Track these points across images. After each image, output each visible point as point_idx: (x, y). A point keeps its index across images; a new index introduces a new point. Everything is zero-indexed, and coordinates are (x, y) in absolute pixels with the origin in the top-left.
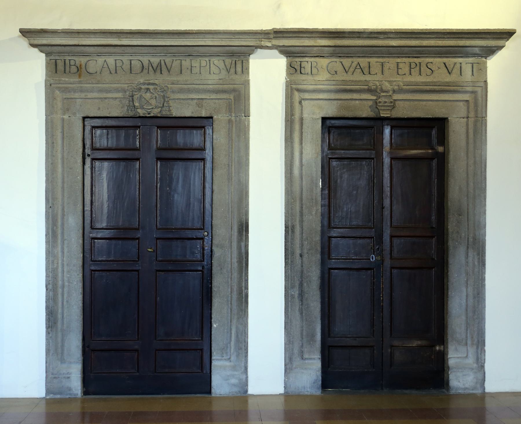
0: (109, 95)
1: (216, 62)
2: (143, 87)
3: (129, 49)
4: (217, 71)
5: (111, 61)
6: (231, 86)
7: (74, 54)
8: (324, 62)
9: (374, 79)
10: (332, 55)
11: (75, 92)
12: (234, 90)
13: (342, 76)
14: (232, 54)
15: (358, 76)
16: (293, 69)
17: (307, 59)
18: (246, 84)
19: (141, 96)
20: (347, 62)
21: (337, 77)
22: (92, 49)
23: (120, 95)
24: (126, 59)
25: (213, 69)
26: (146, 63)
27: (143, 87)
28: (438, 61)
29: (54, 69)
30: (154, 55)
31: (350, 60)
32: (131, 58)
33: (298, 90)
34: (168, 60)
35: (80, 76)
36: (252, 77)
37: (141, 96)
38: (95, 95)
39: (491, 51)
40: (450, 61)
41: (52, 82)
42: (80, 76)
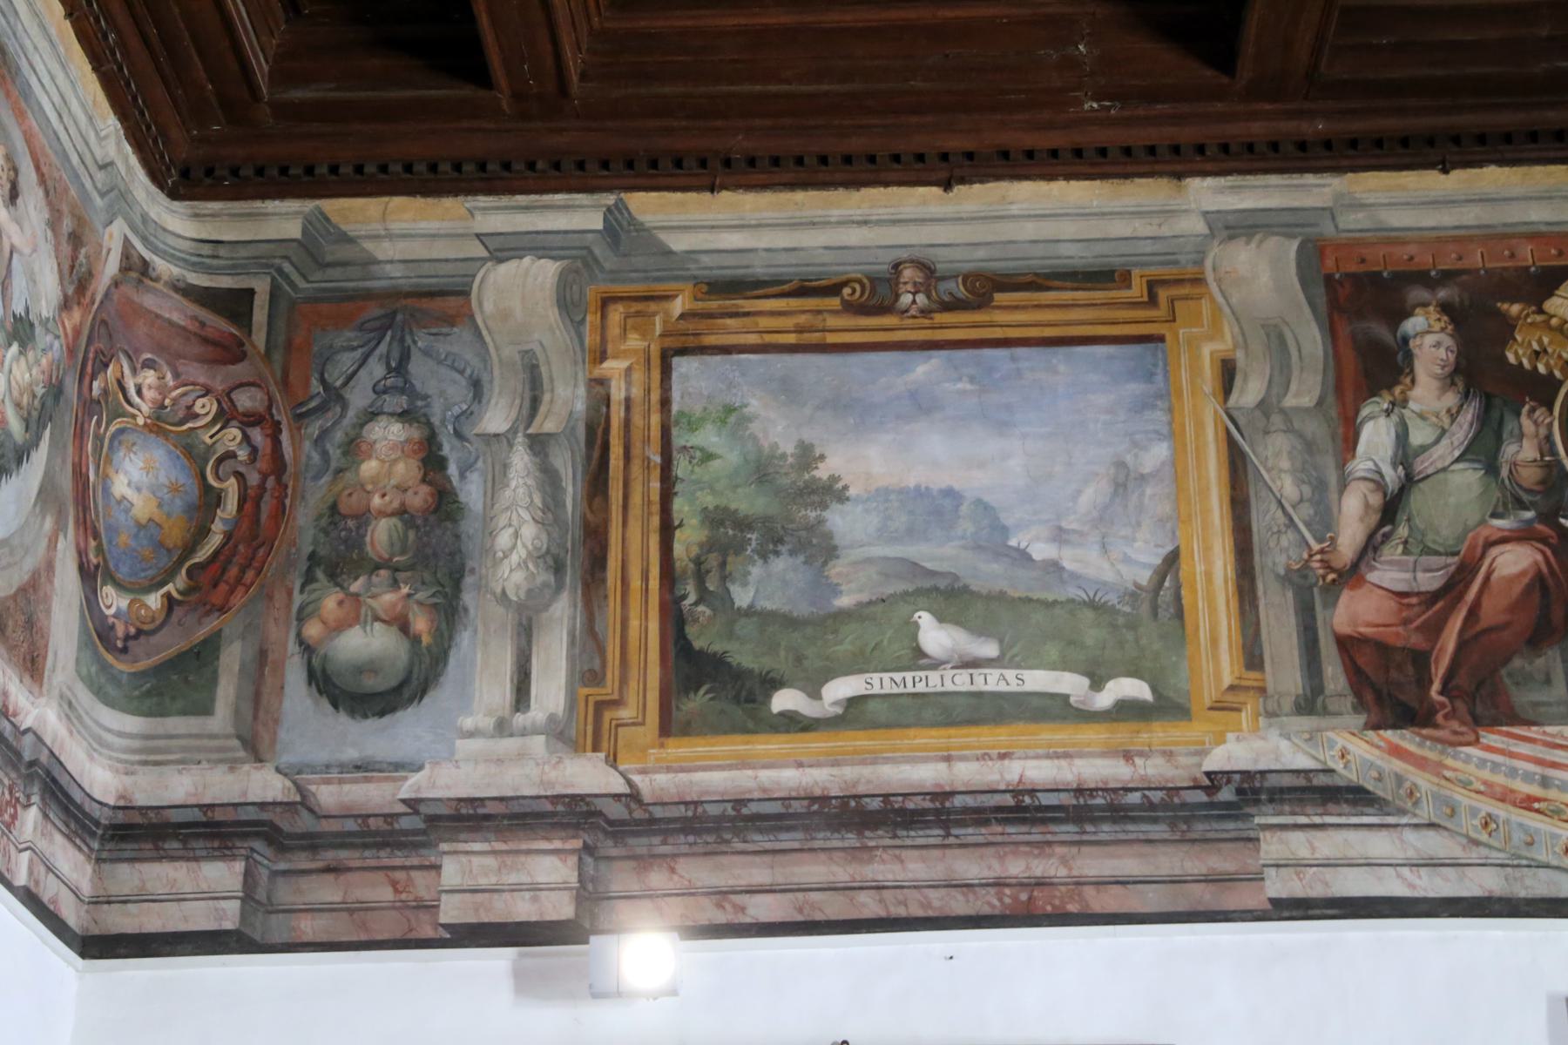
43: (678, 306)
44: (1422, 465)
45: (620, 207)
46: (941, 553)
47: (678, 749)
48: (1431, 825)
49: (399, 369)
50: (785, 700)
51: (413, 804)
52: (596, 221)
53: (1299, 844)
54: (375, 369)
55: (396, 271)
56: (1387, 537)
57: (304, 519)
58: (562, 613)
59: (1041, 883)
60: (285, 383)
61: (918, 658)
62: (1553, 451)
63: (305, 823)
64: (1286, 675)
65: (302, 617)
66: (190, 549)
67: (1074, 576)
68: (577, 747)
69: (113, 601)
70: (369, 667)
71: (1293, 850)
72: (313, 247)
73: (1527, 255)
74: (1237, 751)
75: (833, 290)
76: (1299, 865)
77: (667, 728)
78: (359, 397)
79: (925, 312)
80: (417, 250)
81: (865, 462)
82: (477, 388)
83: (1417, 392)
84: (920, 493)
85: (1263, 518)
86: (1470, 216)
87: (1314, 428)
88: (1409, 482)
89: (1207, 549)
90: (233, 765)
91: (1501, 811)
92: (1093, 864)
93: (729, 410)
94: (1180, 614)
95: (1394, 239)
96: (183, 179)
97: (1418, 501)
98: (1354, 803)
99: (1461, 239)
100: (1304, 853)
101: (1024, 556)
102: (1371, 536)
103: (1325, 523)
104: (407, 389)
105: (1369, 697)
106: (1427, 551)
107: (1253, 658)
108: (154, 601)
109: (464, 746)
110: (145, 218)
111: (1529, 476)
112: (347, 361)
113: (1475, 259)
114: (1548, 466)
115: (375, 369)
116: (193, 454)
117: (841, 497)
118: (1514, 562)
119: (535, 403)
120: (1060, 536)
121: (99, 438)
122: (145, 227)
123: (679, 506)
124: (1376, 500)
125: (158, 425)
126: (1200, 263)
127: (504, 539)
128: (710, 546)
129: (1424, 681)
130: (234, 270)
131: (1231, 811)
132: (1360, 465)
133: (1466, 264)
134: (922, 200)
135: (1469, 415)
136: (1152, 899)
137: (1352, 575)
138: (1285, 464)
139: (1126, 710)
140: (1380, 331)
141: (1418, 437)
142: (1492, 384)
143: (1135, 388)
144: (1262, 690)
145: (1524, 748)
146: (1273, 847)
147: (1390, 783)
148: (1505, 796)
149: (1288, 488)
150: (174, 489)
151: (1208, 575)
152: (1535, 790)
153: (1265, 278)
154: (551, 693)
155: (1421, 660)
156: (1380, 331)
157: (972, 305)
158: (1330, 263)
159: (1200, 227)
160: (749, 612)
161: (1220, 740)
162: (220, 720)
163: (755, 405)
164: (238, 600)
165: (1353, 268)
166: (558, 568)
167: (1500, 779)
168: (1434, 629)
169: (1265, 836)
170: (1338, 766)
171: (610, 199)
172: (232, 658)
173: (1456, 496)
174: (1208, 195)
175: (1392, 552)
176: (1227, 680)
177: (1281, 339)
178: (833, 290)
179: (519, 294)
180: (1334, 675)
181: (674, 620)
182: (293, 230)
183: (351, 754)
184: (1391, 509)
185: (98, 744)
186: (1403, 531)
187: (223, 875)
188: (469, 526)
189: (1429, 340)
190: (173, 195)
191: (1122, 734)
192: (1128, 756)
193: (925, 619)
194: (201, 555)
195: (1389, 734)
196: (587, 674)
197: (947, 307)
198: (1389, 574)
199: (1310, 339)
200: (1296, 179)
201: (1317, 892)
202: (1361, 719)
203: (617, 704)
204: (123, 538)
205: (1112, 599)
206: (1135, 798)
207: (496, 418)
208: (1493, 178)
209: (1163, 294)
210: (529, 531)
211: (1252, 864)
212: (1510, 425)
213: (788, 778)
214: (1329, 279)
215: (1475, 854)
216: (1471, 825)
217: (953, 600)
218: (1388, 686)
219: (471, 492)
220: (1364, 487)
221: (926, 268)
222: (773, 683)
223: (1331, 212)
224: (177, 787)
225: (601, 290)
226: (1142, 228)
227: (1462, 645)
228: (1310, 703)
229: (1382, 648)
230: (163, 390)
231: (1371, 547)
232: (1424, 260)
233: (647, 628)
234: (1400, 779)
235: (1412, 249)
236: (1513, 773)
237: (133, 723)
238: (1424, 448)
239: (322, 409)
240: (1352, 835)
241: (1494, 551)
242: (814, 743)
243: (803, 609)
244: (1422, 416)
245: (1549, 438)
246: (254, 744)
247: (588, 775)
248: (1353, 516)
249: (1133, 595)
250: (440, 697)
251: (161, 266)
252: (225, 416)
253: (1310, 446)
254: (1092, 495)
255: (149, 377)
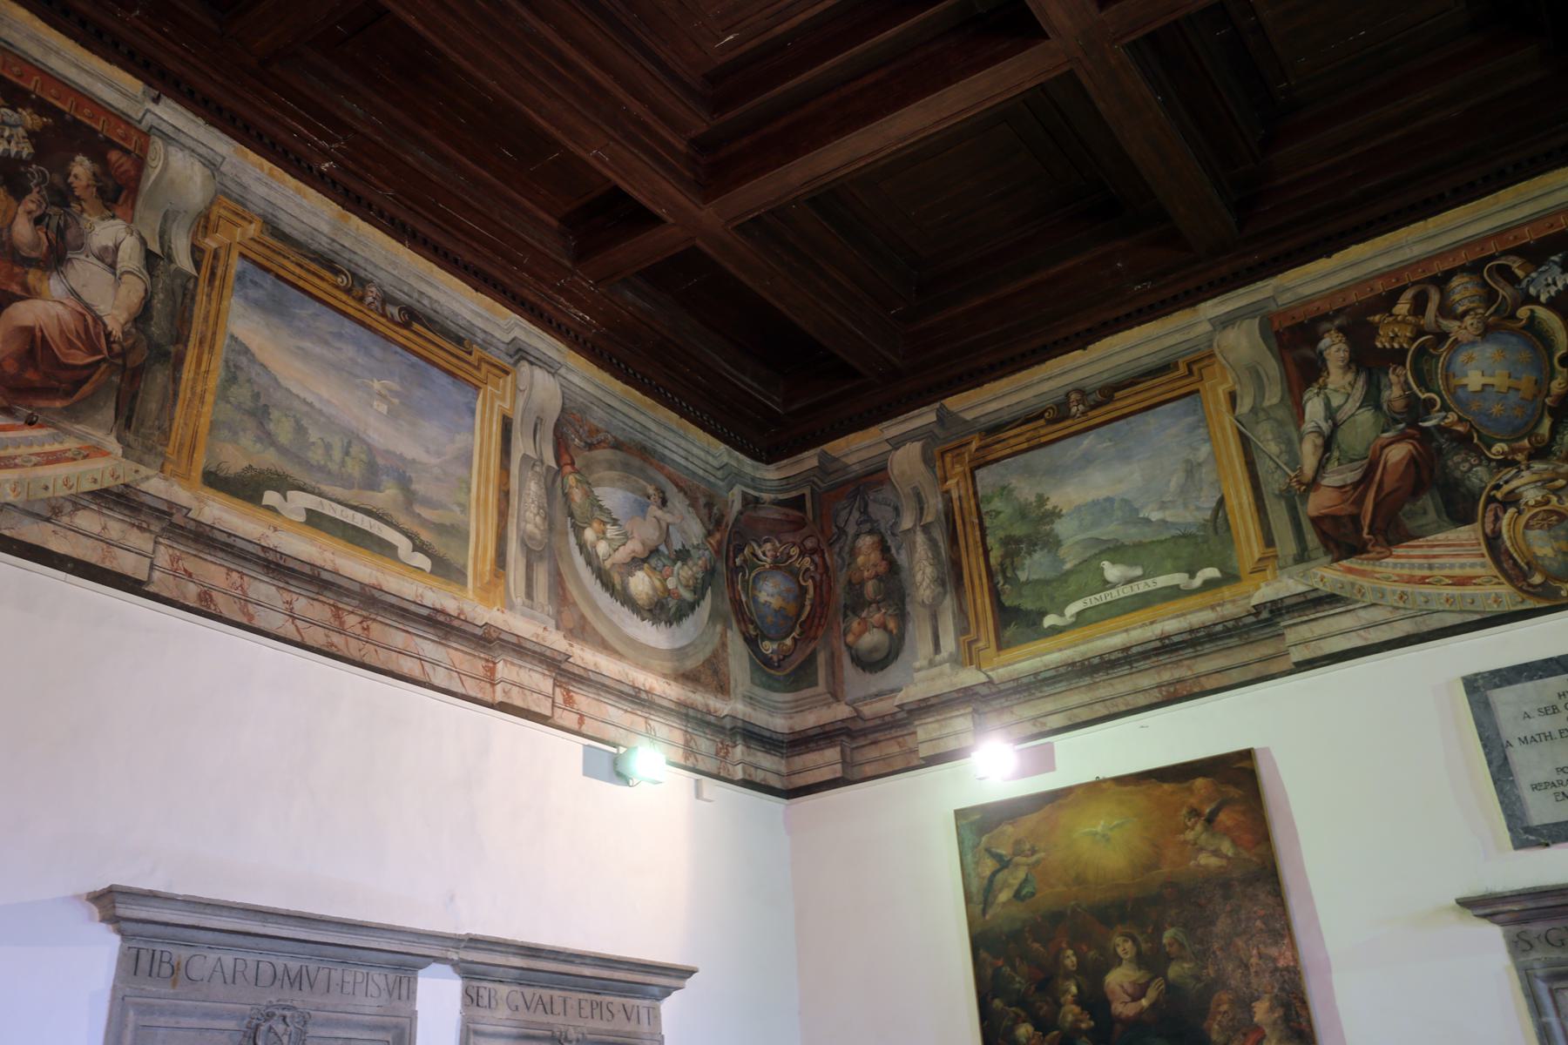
0: (217, 1024)
1: (376, 977)
2: (278, 1012)
3: (266, 943)
4: (376, 993)
5: (228, 959)
6: (395, 1020)
7: (174, 941)
8: (503, 990)
9: (558, 1021)
10: (519, 982)
11: (162, 1013)
12: (396, 1027)
13: (523, 1015)
14: (399, 967)
15: (541, 1017)
16: (471, 999)
17: (484, 984)
18: (412, 1017)
19: (270, 1028)
20: (528, 992)
21: (518, 1016)
22: (210, 936)
23: (232, 1025)
24: (251, 958)
25: (372, 989)
26: (280, 970)
27: (278, 1012)
28: (618, 1000)
29: (134, 966)
30: (294, 955)
31: (532, 990)
32: (259, 958)
33: (476, 1033)
34: (312, 967)
35: (174, 984)
36: (419, 1007)
37: (270, 1028)
38: (195, 1022)
39: (667, 991)
40: (630, 1002)
41: (128, 991)
42: (174, 984)
43: (974, 446)
44: (1340, 416)
45: (943, 406)
46: (1110, 530)
47: (1007, 655)
48: (1373, 605)
49: (864, 511)
50: (1049, 621)
51: (900, 706)
52: (932, 417)
53: (1304, 631)
54: (856, 514)
55: (856, 467)
56: (1328, 459)
57: (840, 589)
58: (948, 603)
59: (1180, 681)
60: (822, 531)
61: (1106, 585)
62: (1410, 388)
63: (860, 725)
64: (1286, 544)
65: (845, 635)
66: (799, 615)
67: (1173, 524)
68: (963, 665)
69: (769, 647)
70: (874, 649)
71: (1301, 635)
72: (823, 469)
73: (1380, 287)
74: (1266, 592)
75: (1040, 416)
76: (1305, 642)
77: (1000, 648)
78: (851, 530)
79: (1083, 413)
80: (865, 455)
81: (1068, 495)
82: (897, 510)
83: (1331, 378)
84: (1095, 503)
85: (1264, 467)
86: (1347, 276)
87: (1281, 414)
88: (1336, 426)
89: (1238, 492)
90: (828, 705)
91: (1408, 588)
92: (1203, 666)
93: (1004, 488)
94: (1228, 528)
95: (1307, 301)
96: (769, 454)
97: (1343, 436)
98: (1330, 603)
99: (1343, 289)
100: (1308, 635)
101: (1147, 521)
102: (1320, 461)
103: (1295, 461)
104: (870, 520)
105: (1332, 545)
106: (1352, 461)
107: (1269, 541)
108: (788, 642)
109: (918, 676)
110: (753, 479)
111: (1399, 405)
112: (844, 514)
113: (1353, 298)
114: (1408, 397)
115: (856, 514)
116: (793, 573)
117: (1060, 515)
118: (1398, 453)
119: (922, 509)
120: (1163, 506)
121: (745, 582)
122: (755, 483)
123: (990, 540)
124: (1319, 441)
125: (776, 566)
126: (1211, 346)
127: (919, 577)
128: (1004, 557)
129: (1359, 530)
130: (796, 488)
131: (1269, 623)
132: (1308, 426)
133: (1347, 302)
134: (1077, 357)
135: (1360, 383)
136: (1236, 676)
137: (1313, 484)
138: (1270, 436)
139: (1209, 584)
140: (1308, 352)
141: (1335, 402)
142: (1369, 361)
143: (1190, 419)
144: (1276, 557)
145: (1417, 552)
146: (1291, 636)
147: (1348, 587)
148: (1410, 580)
149: (1273, 448)
150: (788, 591)
151: (1240, 504)
152: (1426, 573)
153: (1244, 343)
154: (949, 643)
155: (1355, 519)
156: (1307, 352)
157: (1104, 402)
158: (1276, 325)
159: (1207, 327)
160: (1028, 582)
161: (1258, 588)
162: (821, 687)
163: (1014, 483)
164: (820, 633)
165: (1288, 323)
166: (943, 584)
167: (1406, 572)
168: (1359, 502)
169: (1287, 631)
170: (1320, 586)
171: (937, 405)
172: (821, 659)
173: (1361, 426)
174: (1212, 308)
175: (1333, 466)
176: (1257, 556)
177: (1257, 372)
178: (1040, 416)
179: (907, 462)
180: (1312, 539)
181: (995, 594)
182: (815, 462)
183: (873, 690)
184: (1328, 443)
185: (773, 709)
186: (1336, 454)
187: (832, 754)
188: (904, 575)
189: (1334, 349)
190: (768, 463)
191: (1208, 597)
192: (1213, 608)
193: (1106, 564)
194: (803, 617)
195: (1345, 563)
196: (962, 630)
197: (1093, 408)
198: (1331, 479)
199: (1272, 367)
200: (1253, 287)
201: (1319, 653)
202: (1329, 558)
203: (977, 640)
204: (770, 619)
205: (1194, 530)
206: (1219, 628)
207: (907, 523)
208: (1356, 251)
209: (1195, 368)
210: (929, 570)
211: (1283, 647)
212: (1384, 381)
213: (1055, 658)
214: (1277, 333)
215: (1398, 615)
216: (1392, 600)
217: (1116, 551)
218: (1341, 538)
219: (902, 558)
220: (1312, 436)
221: (1081, 391)
222: (1043, 614)
223: (1273, 298)
224: (810, 720)
225: (941, 448)
226: (1178, 338)
227: (1376, 505)
228: (1302, 557)
229: (1334, 518)
230: (775, 550)
231: (1321, 467)
232: (1325, 307)
233: (984, 601)
234: (1353, 584)
235: (1317, 304)
236: (1412, 566)
237: (789, 696)
238: (1340, 407)
239: (839, 538)
240: (1331, 620)
241: (1386, 451)
242: (1066, 638)
243: (1051, 574)
244: (1336, 391)
245: (1406, 382)
246: (835, 695)
247: (970, 677)
248: (1309, 455)
249: (1204, 526)
250: (904, 656)
251: (765, 496)
252: (802, 554)
253: (1281, 423)
254: (1175, 482)
255: (768, 546)
